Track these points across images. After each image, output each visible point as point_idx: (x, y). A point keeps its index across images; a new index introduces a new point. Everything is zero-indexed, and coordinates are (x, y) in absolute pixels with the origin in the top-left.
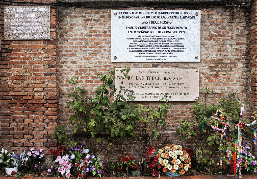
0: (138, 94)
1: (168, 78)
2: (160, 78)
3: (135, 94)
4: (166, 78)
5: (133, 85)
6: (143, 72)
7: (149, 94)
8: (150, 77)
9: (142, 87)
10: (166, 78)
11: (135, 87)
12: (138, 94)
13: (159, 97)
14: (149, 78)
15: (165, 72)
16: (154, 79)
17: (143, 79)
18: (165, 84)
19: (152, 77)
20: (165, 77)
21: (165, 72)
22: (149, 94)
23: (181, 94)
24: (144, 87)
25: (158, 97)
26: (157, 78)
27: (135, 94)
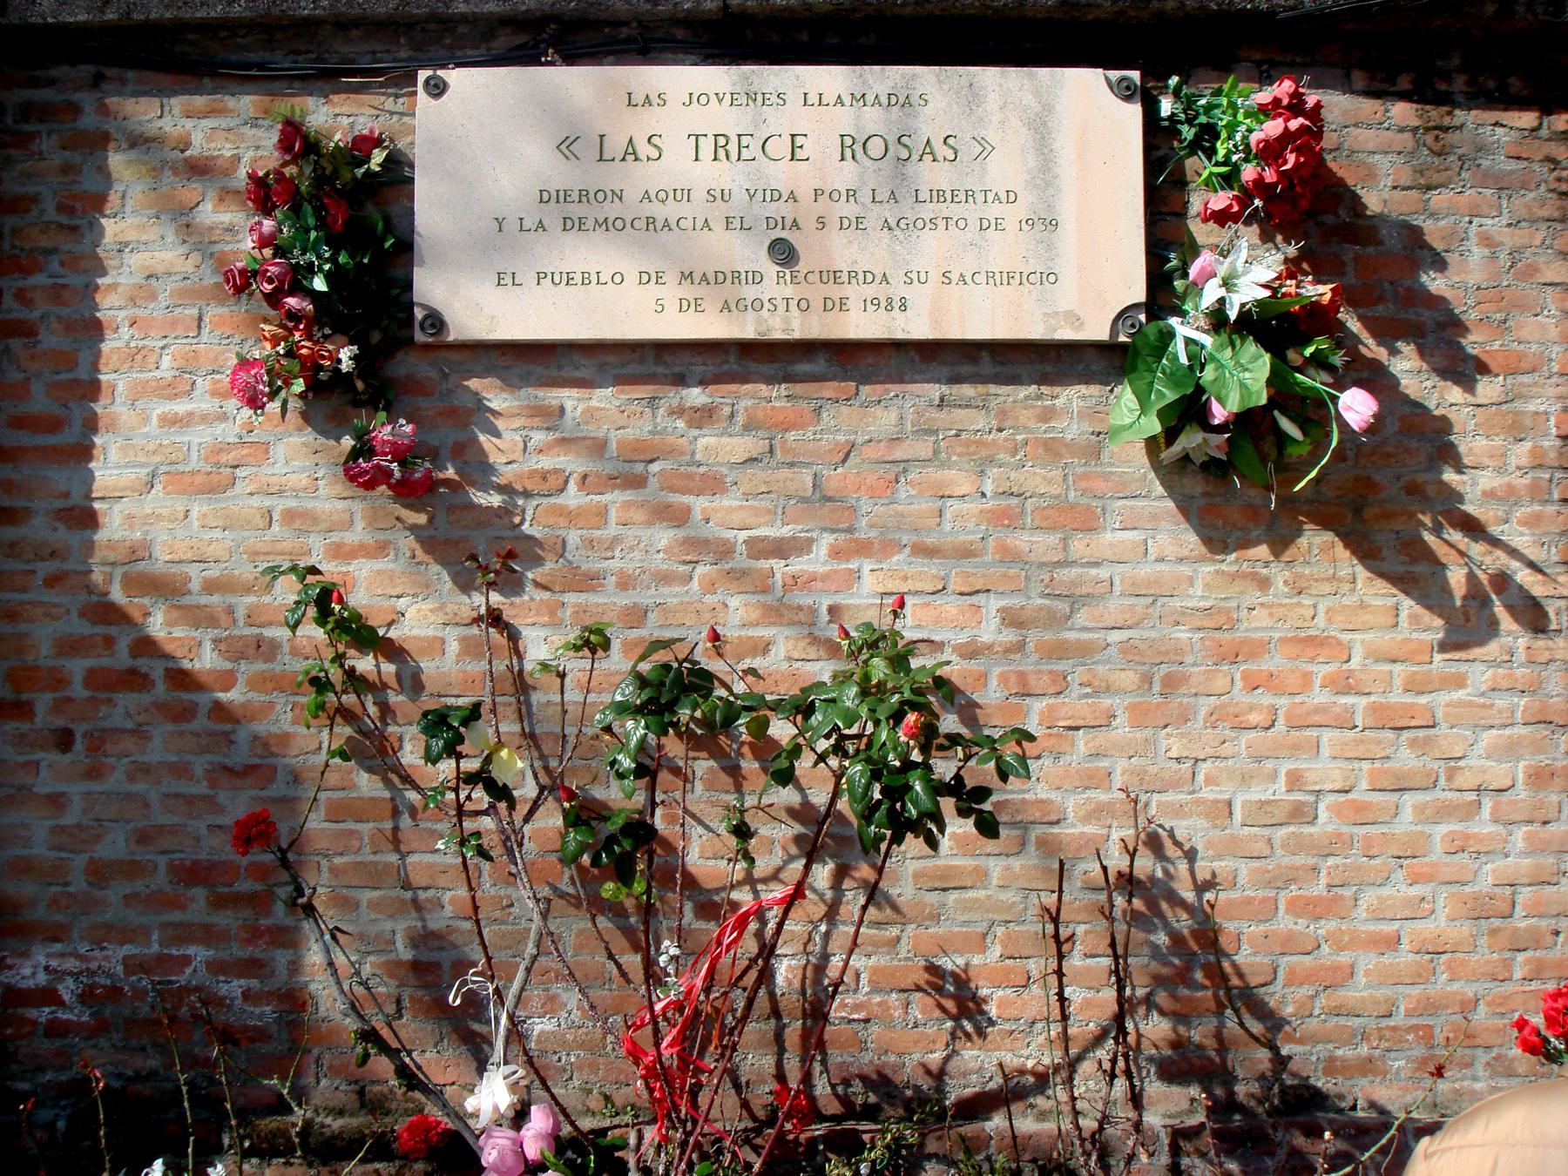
0: (618, 279)
1: (876, 147)
2: (809, 148)
3: (594, 278)
4: (858, 148)
5: (576, 210)
6: (655, 100)
7: (712, 280)
8: (722, 141)
9: (651, 221)
10: (858, 148)
11: (590, 224)
12: (618, 279)
13: (804, 305)
14: (707, 146)
15: (847, 100)
16: (755, 150)
17: (654, 154)
18: (851, 194)
19: (734, 140)
20: (848, 141)
21: (847, 100)
22: (712, 280)
23: (990, 276)
24: (666, 224)
25: (793, 304)
26: (780, 147)
27: (594, 278)
